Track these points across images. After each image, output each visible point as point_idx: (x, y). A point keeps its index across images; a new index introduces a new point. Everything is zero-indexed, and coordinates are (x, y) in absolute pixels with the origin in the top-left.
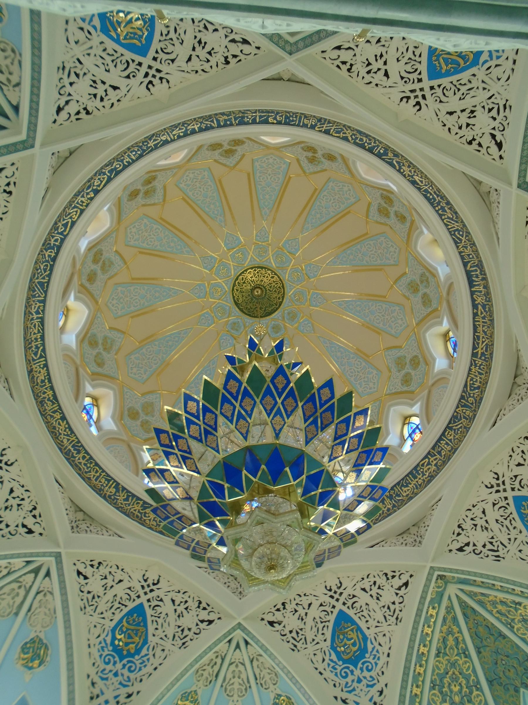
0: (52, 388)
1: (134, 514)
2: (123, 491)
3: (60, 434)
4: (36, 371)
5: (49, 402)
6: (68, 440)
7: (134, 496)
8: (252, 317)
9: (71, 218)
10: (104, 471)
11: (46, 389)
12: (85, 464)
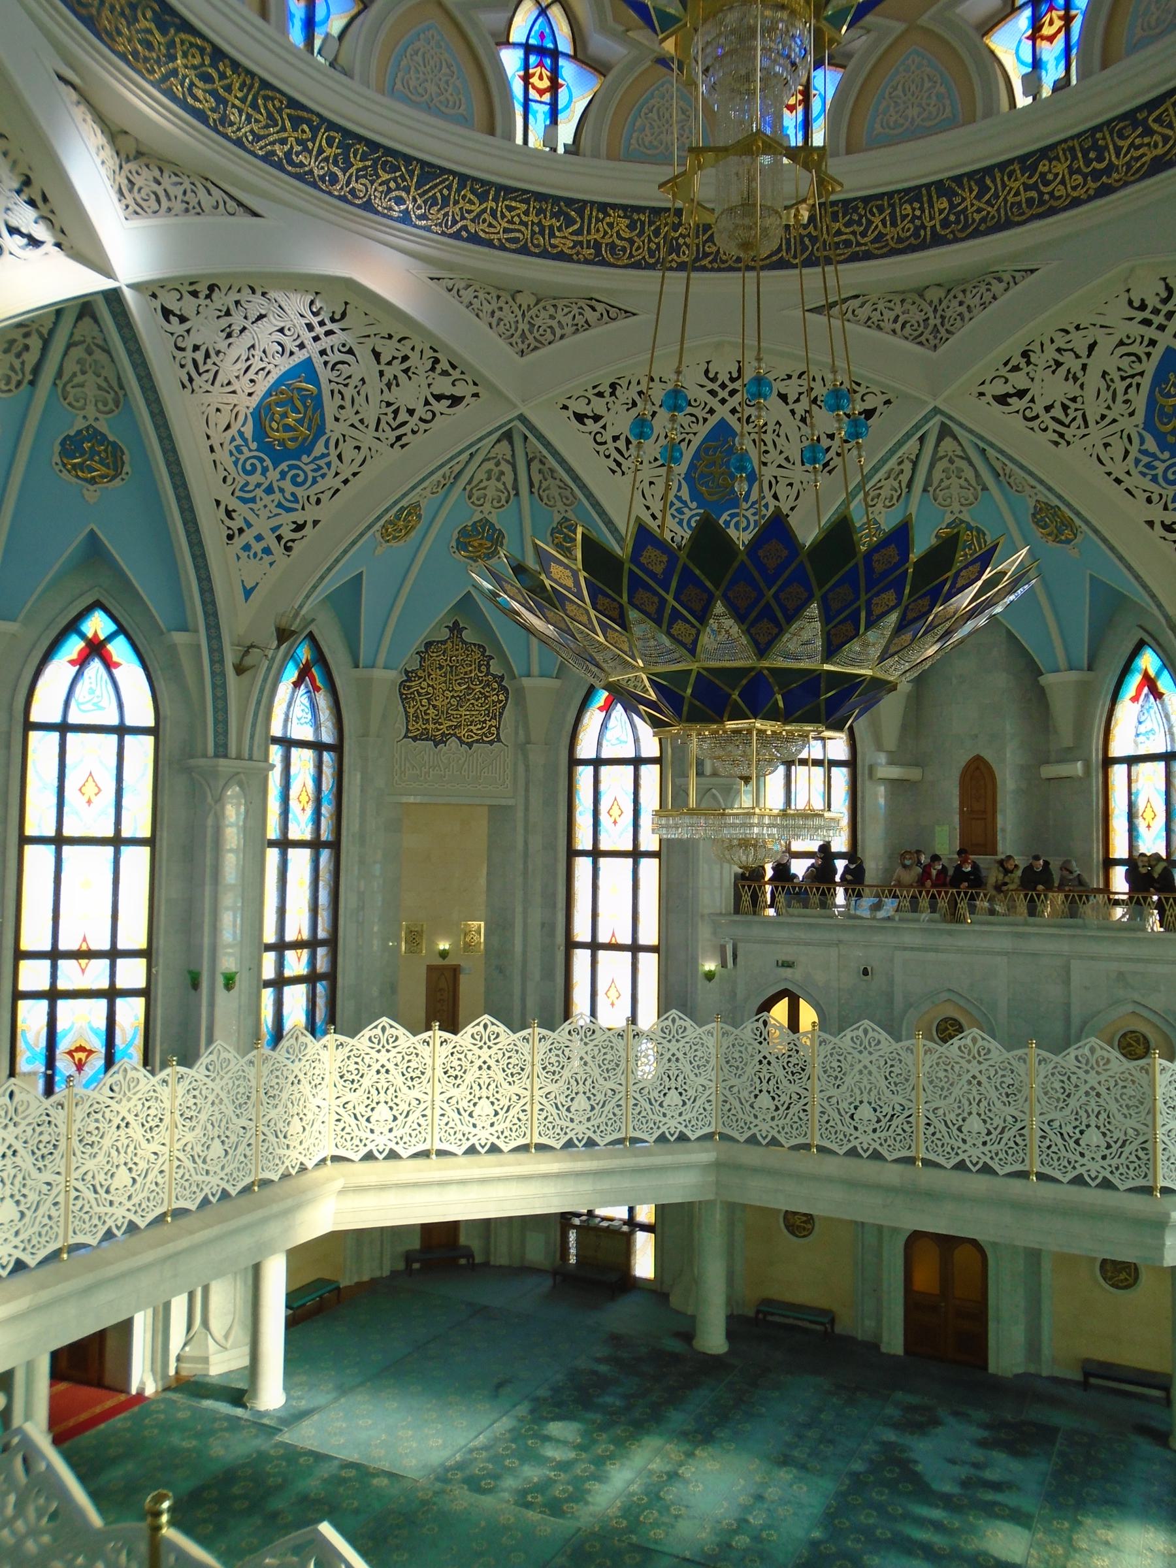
1: (1019, 203)
2: (961, 186)
4: (606, 233)
7: (988, 170)
10: (890, 195)
11: (651, 223)
12: (847, 225)
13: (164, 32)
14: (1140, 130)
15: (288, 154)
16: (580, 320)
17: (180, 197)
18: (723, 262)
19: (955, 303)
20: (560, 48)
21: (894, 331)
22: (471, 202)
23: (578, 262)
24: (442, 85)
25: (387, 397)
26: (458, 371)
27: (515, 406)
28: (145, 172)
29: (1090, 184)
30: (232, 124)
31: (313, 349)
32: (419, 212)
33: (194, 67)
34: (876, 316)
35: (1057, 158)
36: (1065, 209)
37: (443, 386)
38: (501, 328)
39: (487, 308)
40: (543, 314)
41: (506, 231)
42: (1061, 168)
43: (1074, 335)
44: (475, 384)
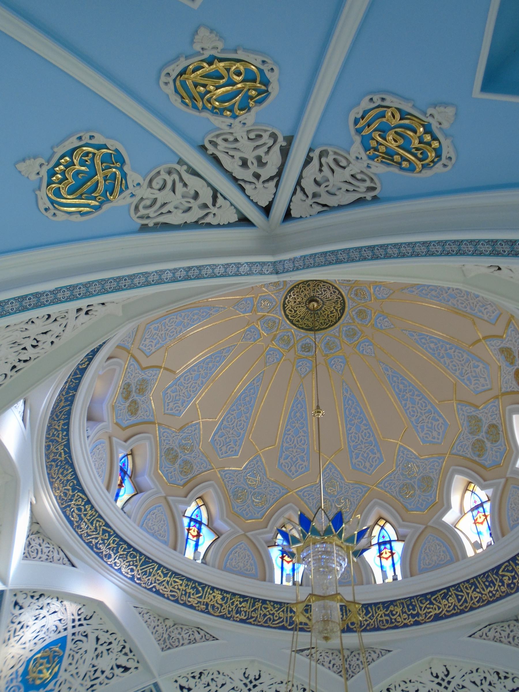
0: (234, 594)
1: (383, 621)
3: (273, 614)
4: (211, 600)
5: (243, 604)
6: (283, 611)
7: (370, 605)
8: (334, 325)
9: (100, 526)
13: (73, 492)
14: (428, 602)
15: (97, 543)
16: (192, 637)
17: (47, 553)
18: (259, 622)
19: (355, 659)
20: (203, 522)
21: (329, 668)
22: (160, 576)
23: (198, 610)
24: (160, 527)
25: (95, 662)
26: (132, 654)
27: (154, 677)
28: (37, 541)
29: (411, 619)
30: (81, 528)
31: (70, 631)
32: (139, 577)
33: (77, 505)
34: (321, 659)
35: (397, 605)
36: (402, 627)
37: (123, 661)
38: (157, 635)
39: (153, 624)
40: (176, 632)
41: (171, 591)
42: (399, 610)
43: (409, 684)
44: (138, 662)
